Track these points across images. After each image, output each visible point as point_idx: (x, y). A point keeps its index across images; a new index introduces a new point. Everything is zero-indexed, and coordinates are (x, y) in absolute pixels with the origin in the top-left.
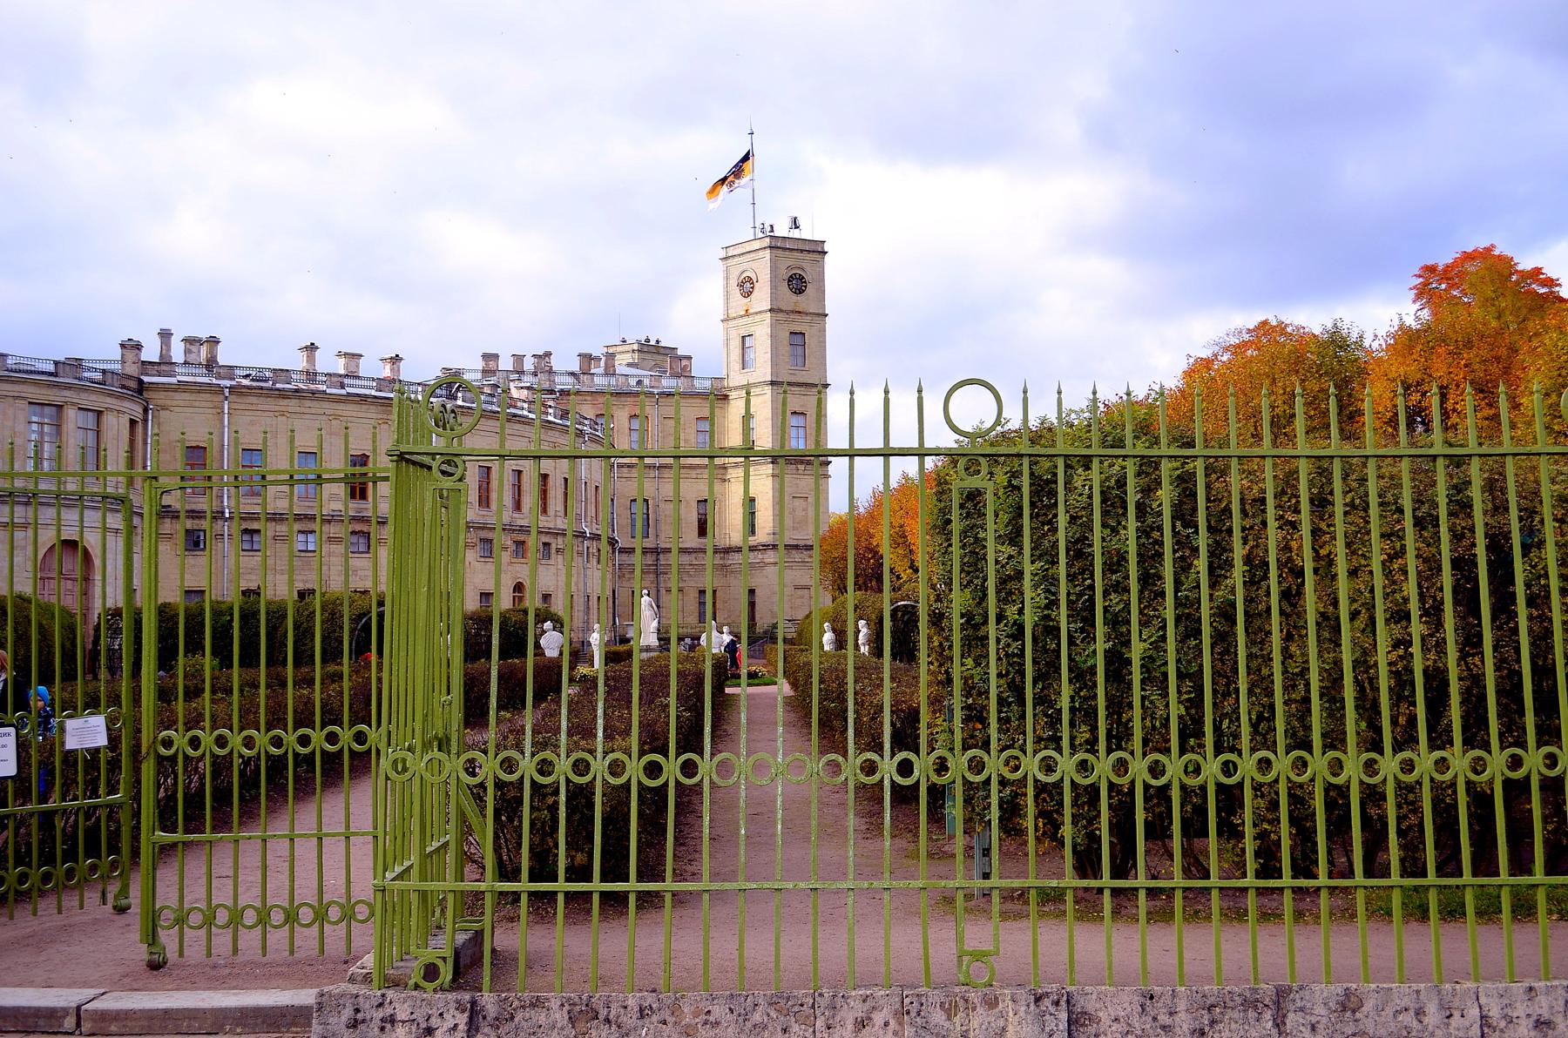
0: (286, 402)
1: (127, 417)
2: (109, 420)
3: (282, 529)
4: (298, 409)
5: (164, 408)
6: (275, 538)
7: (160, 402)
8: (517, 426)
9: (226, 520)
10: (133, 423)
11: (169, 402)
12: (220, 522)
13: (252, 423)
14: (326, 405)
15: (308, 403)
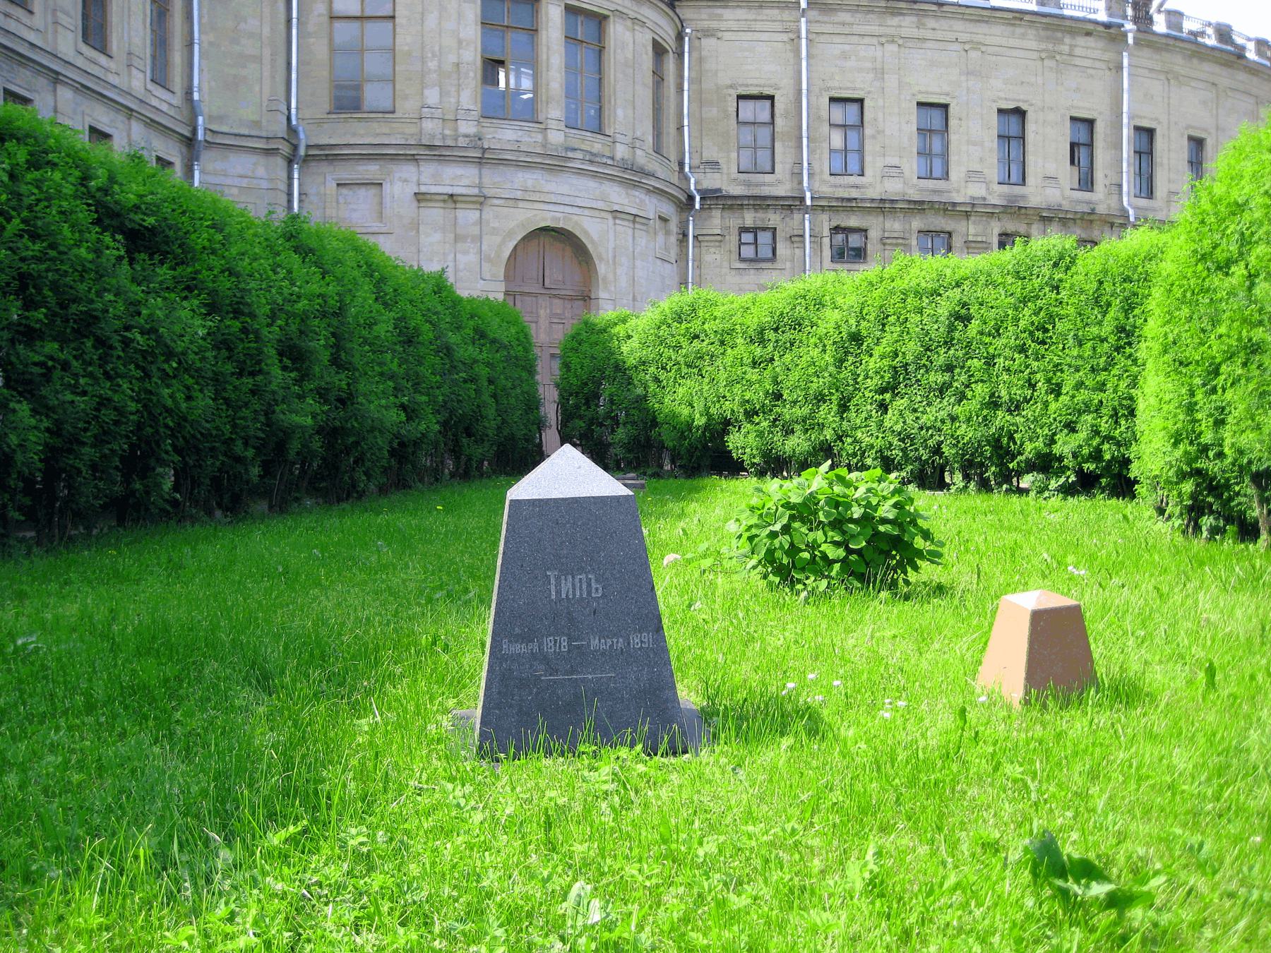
0: (895, 21)
1: (649, 36)
2: (617, 32)
3: (895, 225)
4: (915, 33)
5: (709, 33)
6: (883, 241)
7: (706, 24)
8: (1242, 76)
9: (806, 210)
10: (659, 50)
11: (714, 24)
12: (797, 216)
13: (845, 56)
14: (958, 25)
15: (931, 23)
